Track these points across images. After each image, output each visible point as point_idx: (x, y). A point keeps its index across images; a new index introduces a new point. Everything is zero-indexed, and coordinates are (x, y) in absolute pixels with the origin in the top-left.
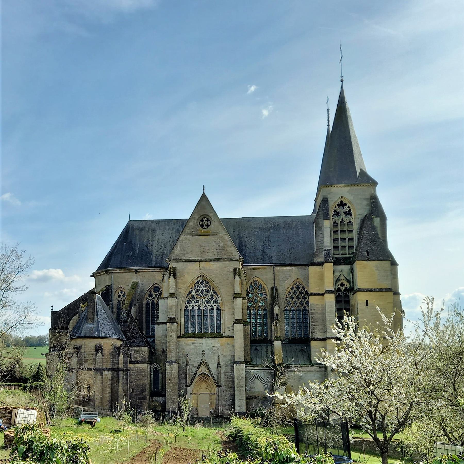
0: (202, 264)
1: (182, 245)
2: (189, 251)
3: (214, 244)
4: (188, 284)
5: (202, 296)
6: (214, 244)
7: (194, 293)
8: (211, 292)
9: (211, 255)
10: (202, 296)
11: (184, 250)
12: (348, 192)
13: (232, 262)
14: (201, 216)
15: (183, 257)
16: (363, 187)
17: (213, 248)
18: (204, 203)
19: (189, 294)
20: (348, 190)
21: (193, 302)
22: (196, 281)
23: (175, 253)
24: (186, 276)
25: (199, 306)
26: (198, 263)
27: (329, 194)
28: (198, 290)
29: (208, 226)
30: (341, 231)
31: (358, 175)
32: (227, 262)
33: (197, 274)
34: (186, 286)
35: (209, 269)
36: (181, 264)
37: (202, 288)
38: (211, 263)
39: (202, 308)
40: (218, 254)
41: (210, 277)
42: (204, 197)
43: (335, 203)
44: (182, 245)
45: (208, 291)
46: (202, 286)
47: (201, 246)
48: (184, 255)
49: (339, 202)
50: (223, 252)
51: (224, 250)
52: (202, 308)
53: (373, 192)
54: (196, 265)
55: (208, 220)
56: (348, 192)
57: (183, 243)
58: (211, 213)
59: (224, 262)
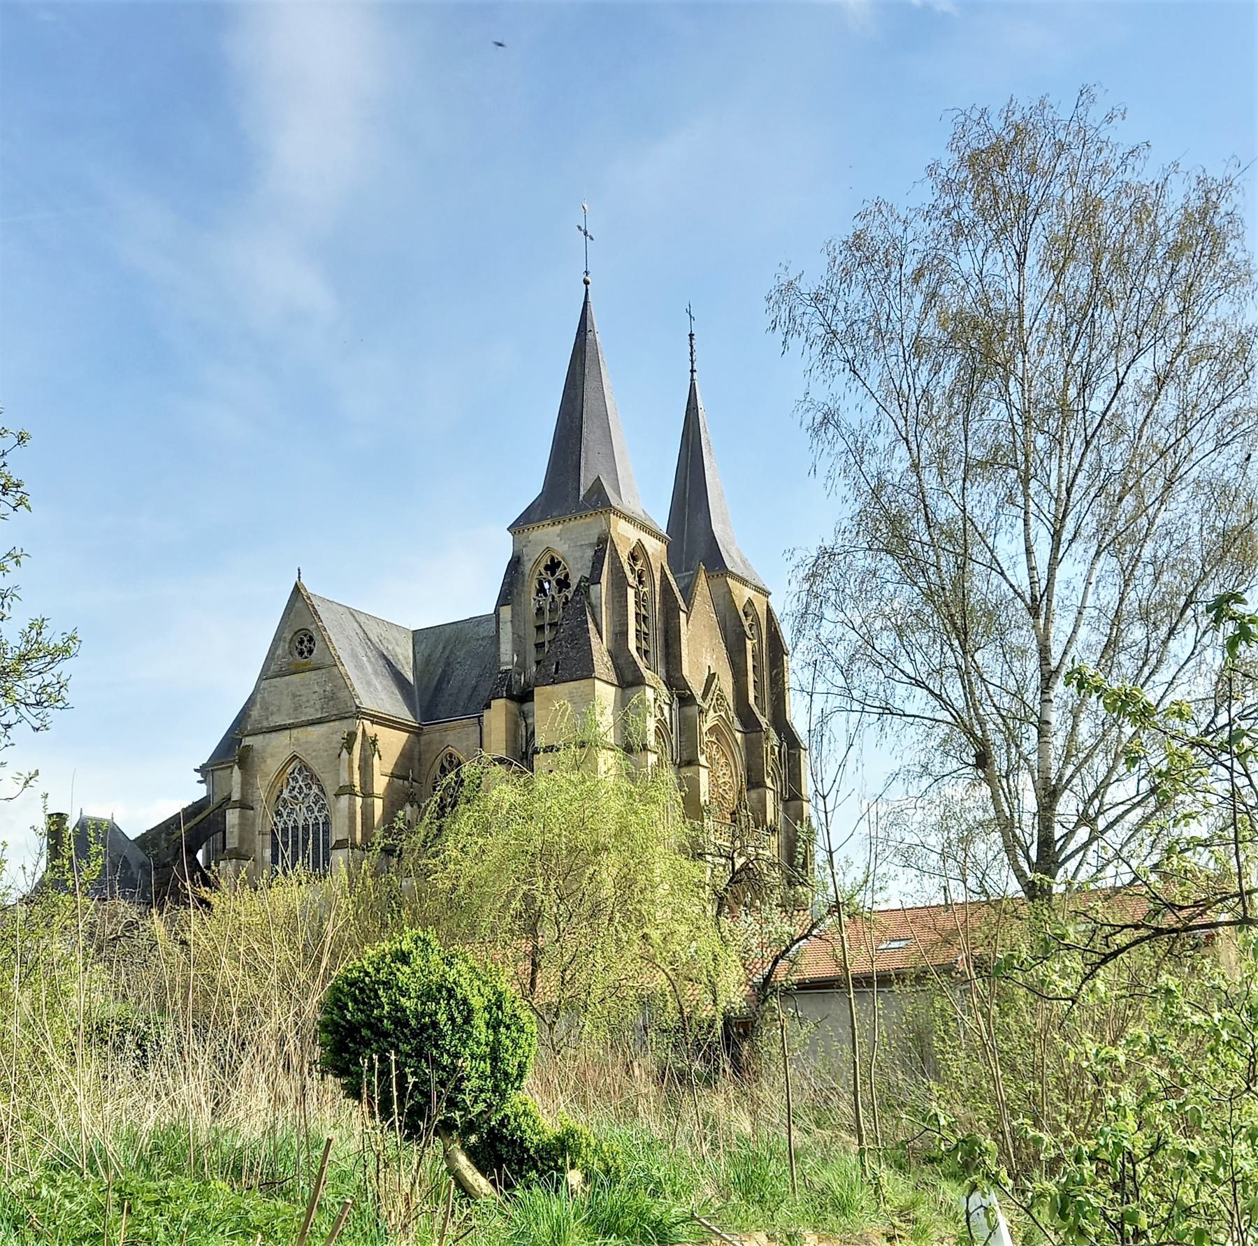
0: (295, 732)
1: (263, 698)
2: (275, 710)
3: (317, 689)
4: (272, 777)
5: (300, 799)
6: (317, 689)
7: (286, 794)
8: (315, 789)
9: (311, 710)
10: (300, 799)
11: (267, 709)
12: (558, 535)
13: (345, 722)
14: (296, 633)
15: (265, 724)
16: (588, 520)
17: (315, 696)
18: (299, 605)
19: (278, 797)
20: (558, 532)
21: (285, 815)
22: (289, 770)
23: (253, 718)
24: (269, 761)
25: (295, 821)
26: (288, 731)
27: (524, 546)
28: (294, 788)
29: (310, 651)
30: (551, 625)
31: (582, 493)
32: (337, 723)
33: (286, 755)
34: (267, 782)
35: (307, 742)
36: (260, 737)
37: (300, 783)
38: (309, 728)
39: (301, 823)
40: (322, 708)
41: (309, 758)
42: (297, 590)
43: (537, 562)
44: (263, 698)
45: (310, 788)
46: (300, 779)
47: (294, 696)
48: (267, 718)
49: (546, 560)
50: (331, 703)
51: (332, 699)
52: (301, 823)
53: (604, 527)
54: (284, 737)
55: (311, 640)
56: (558, 535)
57: (266, 695)
58: (312, 624)
59: (332, 724)
